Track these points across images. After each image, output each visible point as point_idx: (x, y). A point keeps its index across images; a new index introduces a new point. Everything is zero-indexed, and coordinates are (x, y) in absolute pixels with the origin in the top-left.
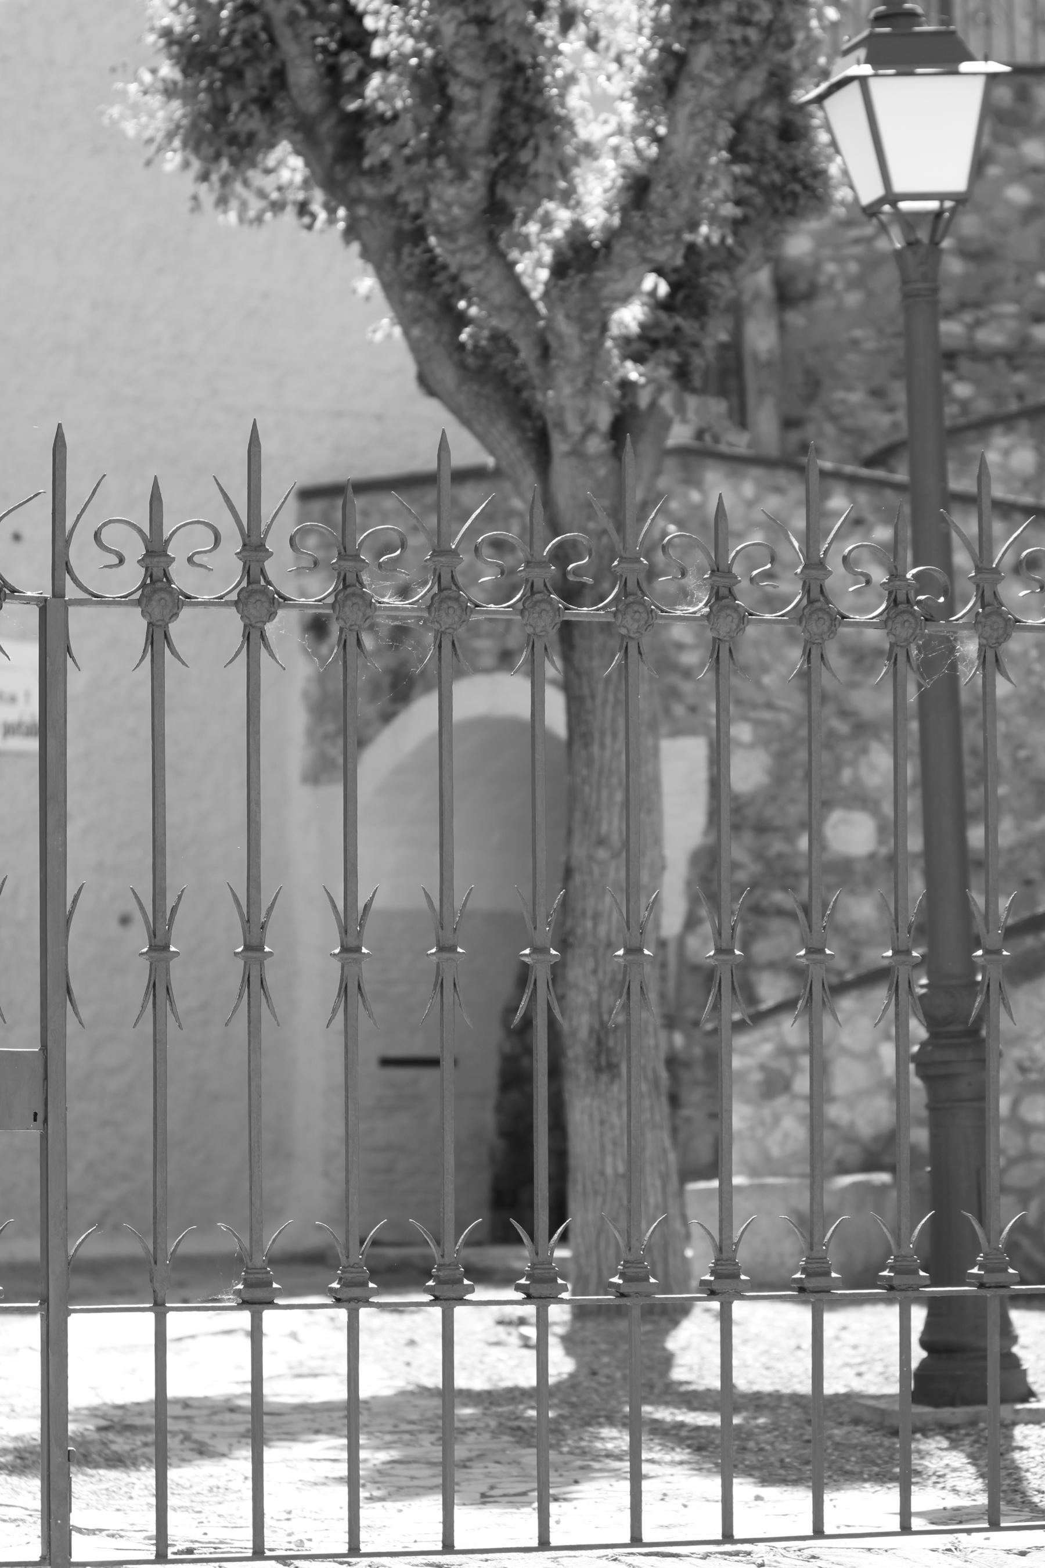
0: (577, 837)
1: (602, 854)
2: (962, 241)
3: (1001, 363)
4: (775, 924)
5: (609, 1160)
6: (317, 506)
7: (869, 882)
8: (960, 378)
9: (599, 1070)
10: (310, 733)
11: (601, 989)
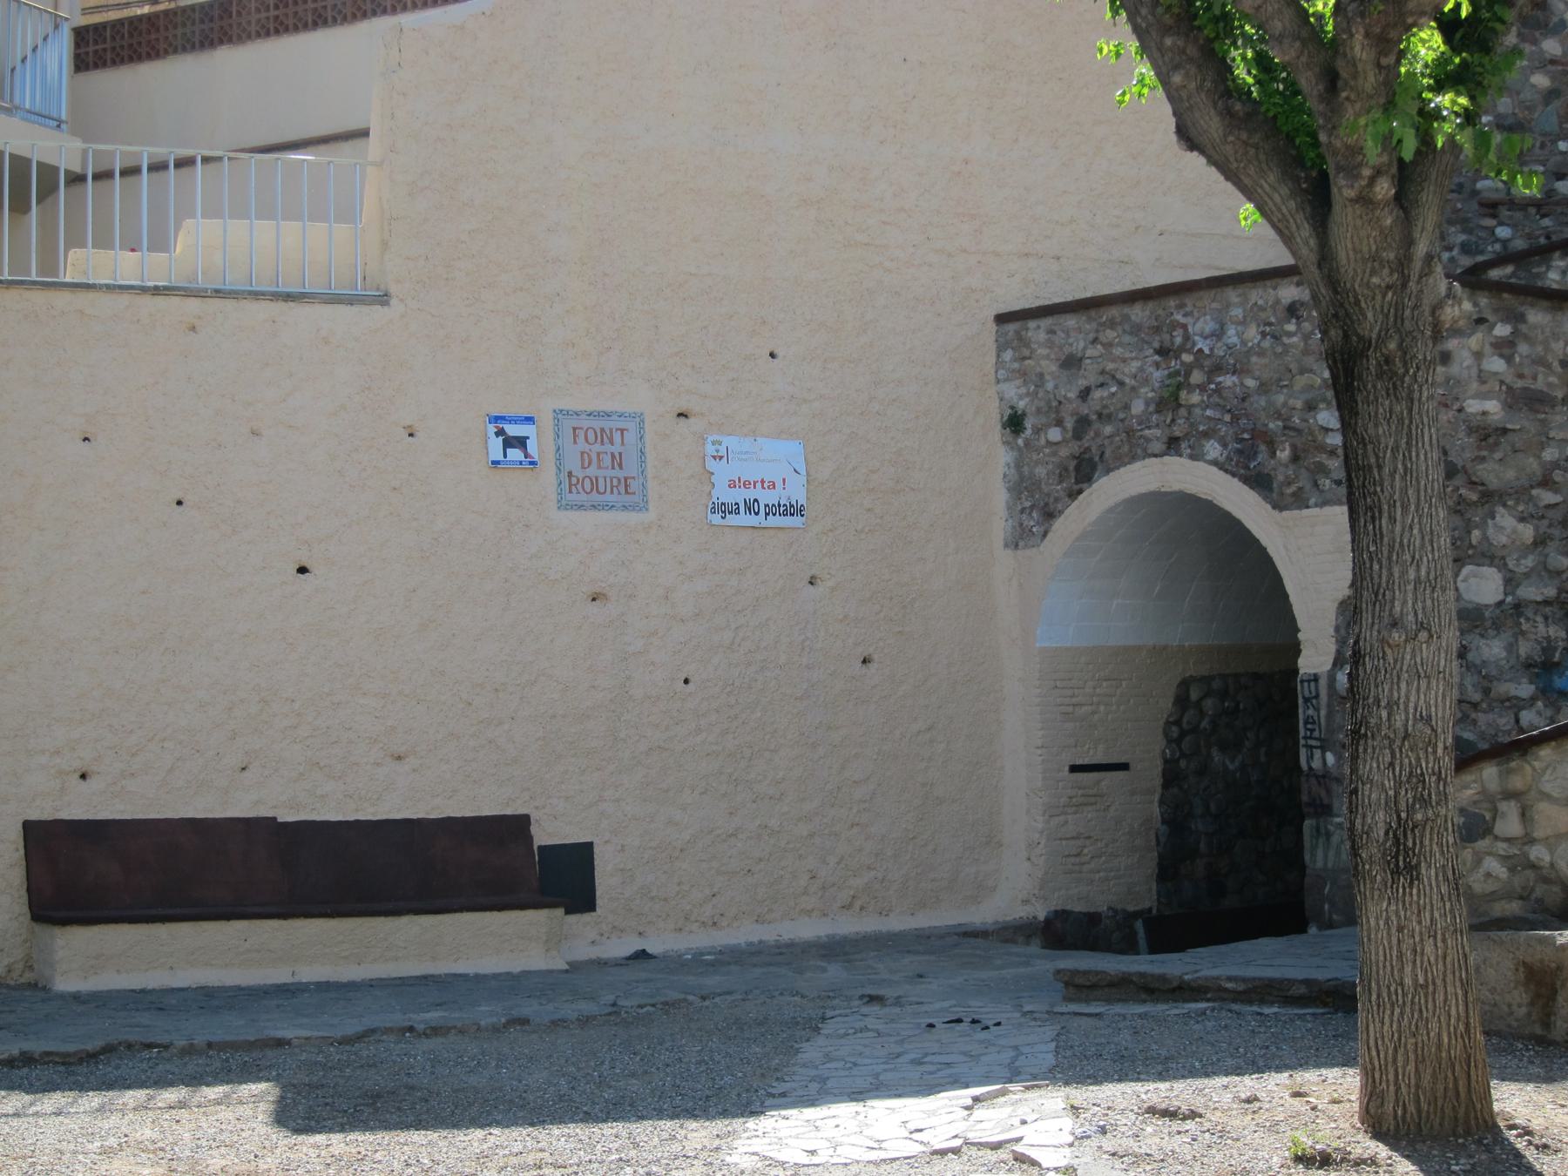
0: (1367, 618)
1: (1396, 636)
2: (1498, 116)
3: (1532, 210)
5: (1408, 969)
6: (1011, 328)
7: (1497, 626)
8: (1501, 224)
9: (1396, 872)
11: (1398, 784)
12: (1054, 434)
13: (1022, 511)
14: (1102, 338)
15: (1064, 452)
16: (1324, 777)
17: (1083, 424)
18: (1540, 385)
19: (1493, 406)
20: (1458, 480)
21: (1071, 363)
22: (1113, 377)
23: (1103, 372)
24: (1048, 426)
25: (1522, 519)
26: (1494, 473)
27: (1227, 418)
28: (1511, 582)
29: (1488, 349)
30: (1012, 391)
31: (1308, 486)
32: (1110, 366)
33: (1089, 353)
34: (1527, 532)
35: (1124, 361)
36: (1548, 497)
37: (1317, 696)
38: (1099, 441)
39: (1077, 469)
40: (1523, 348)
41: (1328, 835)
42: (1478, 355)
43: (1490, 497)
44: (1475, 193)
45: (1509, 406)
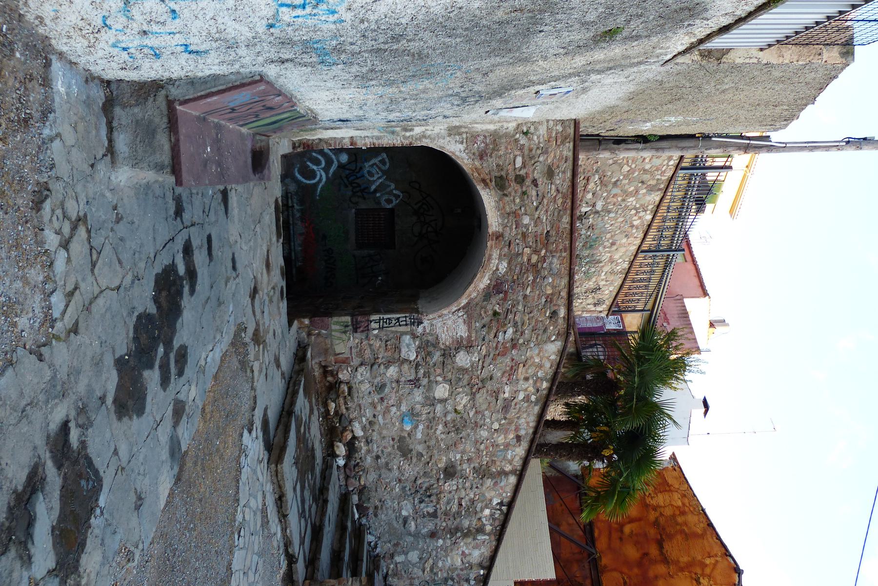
4: (413, 371)
7: (427, 398)
10: (487, 131)
12: (519, 162)
13: (485, 137)
14: (560, 195)
15: (510, 168)
16: (367, 329)
17: (520, 180)
18: (512, 410)
19: (507, 395)
20: (480, 385)
21: (550, 173)
22: (540, 203)
23: (544, 197)
24: (523, 157)
25: (464, 406)
26: (481, 397)
27: (515, 277)
28: (443, 401)
29: (527, 393)
30: (542, 130)
31: (483, 322)
32: (545, 201)
33: (553, 187)
34: (460, 408)
35: (547, 211)
36: (471, 414)
37: (400, 325)
38: (513, 194)
39: (501, 177)
40: (526, 405)
41: (345, 332)
42: (526, 390)
43: (473, 395)
44: (594, 175)
45: (505, 399)
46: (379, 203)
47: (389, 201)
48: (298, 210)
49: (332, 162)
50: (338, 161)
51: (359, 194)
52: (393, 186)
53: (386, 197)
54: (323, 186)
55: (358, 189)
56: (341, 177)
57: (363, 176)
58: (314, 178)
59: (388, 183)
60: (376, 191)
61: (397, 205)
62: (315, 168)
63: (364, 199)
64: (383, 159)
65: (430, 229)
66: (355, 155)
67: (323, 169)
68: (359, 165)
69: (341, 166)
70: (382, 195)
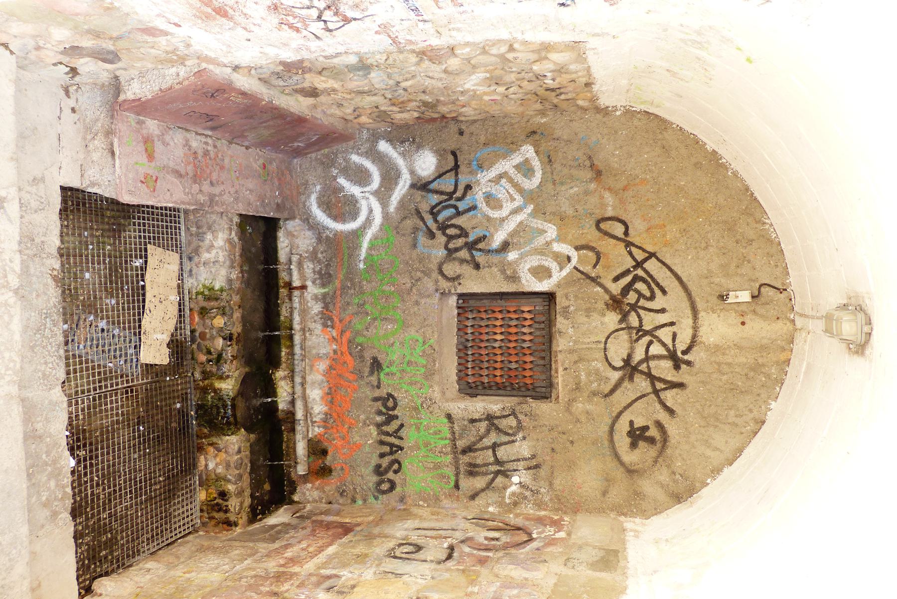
46: (514, 278)
47: (541, 272)
48: (316, 298)
49: (398, 175)
50: (412, 172)
51: (464, 254)
52: (552, 231)
53: (534, 261)
54: (375, 238)
55: (460, 242)
56: (418, 212)
57: (474, 208)
58: (354, 215)
59: (538, 223)
60: (505, 246)
61: (559, 285)
62: (355, 190)
63: (477, 266)
64: (527, 161)
65: (656, 349)
66: (454, 154)
67: (376, 193)
68: (463, 180)
69: (422, 186)
70: (522, 257)
